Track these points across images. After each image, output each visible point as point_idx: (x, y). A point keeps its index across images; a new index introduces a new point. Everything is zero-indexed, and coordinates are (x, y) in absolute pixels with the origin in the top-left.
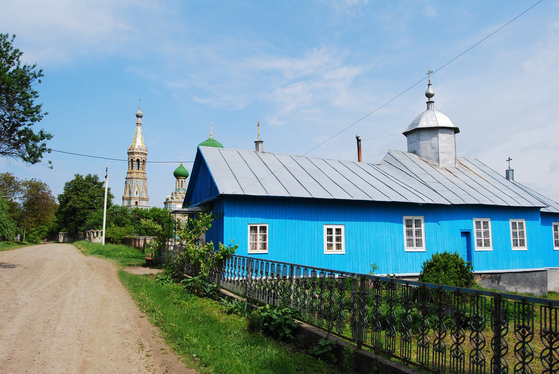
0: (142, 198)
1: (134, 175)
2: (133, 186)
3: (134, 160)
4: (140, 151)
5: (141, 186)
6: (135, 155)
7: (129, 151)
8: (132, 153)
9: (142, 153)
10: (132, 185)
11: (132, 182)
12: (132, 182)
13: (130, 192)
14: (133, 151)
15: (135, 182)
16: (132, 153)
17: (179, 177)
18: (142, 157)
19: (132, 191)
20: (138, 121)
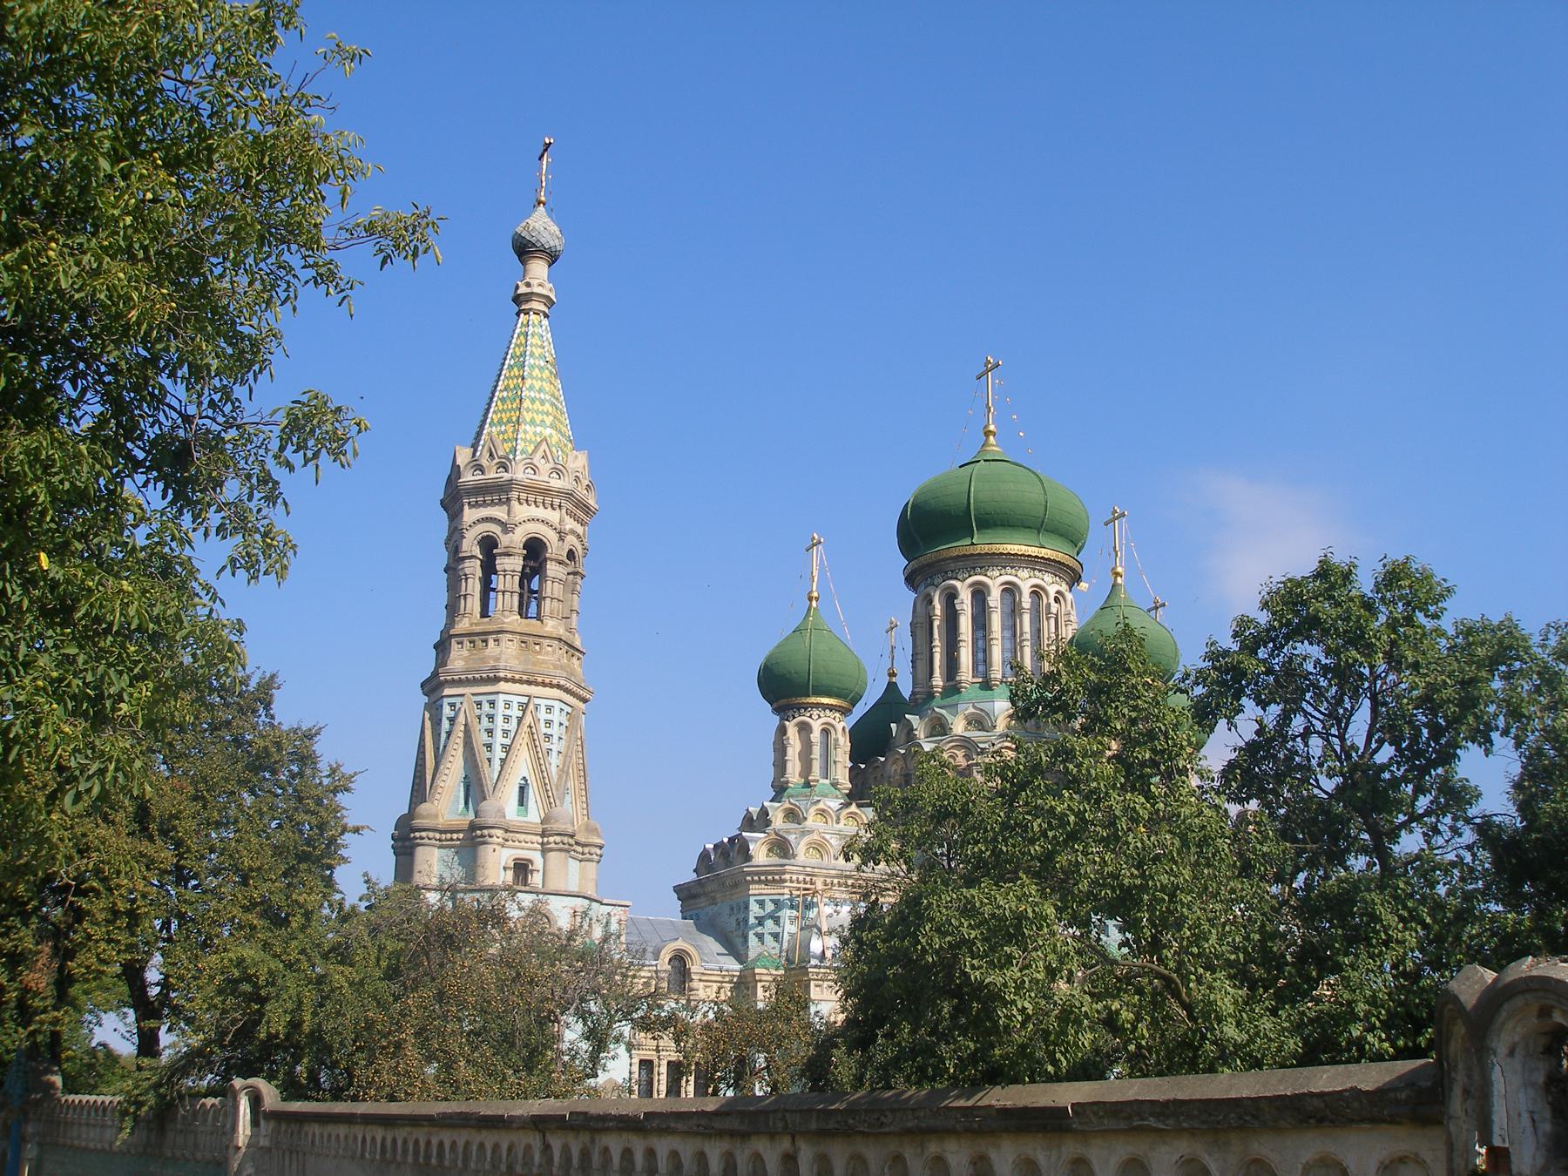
0: (570, 830)
1: (506, 653)
2: (499, 739)
3: (504, 540)
4: (556, 483)
5: (555, 746)
6: (514, 503)
7: (469, 478)
8: (499, 492)
9: (569, 495)
10: (490, 732)
11: (492, 703)
12: (486, 707)
13: (474, 788)
14: (507, 476)
15: (515, 712)
16: (499, 492)
17: (813, 700)
18: (568, 527)
19: (490, 773)
20: (532, 282)
